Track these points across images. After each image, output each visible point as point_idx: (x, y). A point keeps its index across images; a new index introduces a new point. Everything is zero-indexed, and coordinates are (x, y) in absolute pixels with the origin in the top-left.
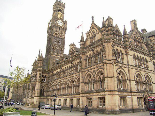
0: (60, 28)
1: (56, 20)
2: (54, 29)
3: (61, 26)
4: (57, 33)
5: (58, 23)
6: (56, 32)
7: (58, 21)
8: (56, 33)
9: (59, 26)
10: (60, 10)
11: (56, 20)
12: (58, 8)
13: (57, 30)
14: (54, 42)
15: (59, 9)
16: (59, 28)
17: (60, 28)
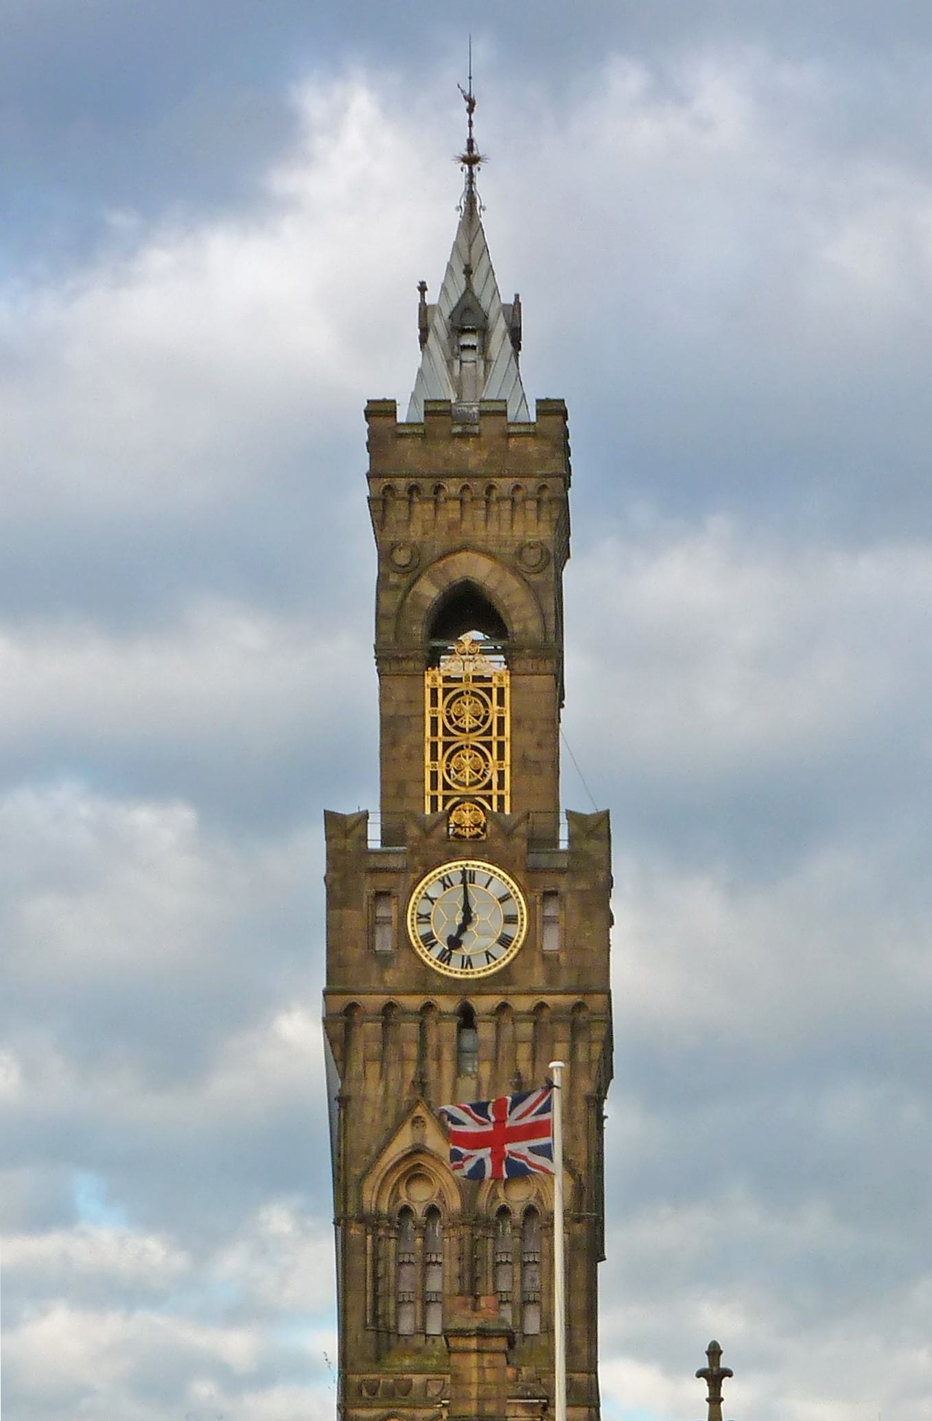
0: (467, 1018)
1: (383, 882)
2: (373, 1089)
3: (482, 986)
4: (434, 1141)
5: (415, 931)
6: (404, 1141)
7: (415, 904)
8: (418, 1150)
9: (454, 986)
10: (466, 609)
11: (383, 882)
12: (413, 571)
13: (421, 1084)
14: (406, 1325)
15: (429, 591)
16: (450, 1027)
17: (467, 1018)
